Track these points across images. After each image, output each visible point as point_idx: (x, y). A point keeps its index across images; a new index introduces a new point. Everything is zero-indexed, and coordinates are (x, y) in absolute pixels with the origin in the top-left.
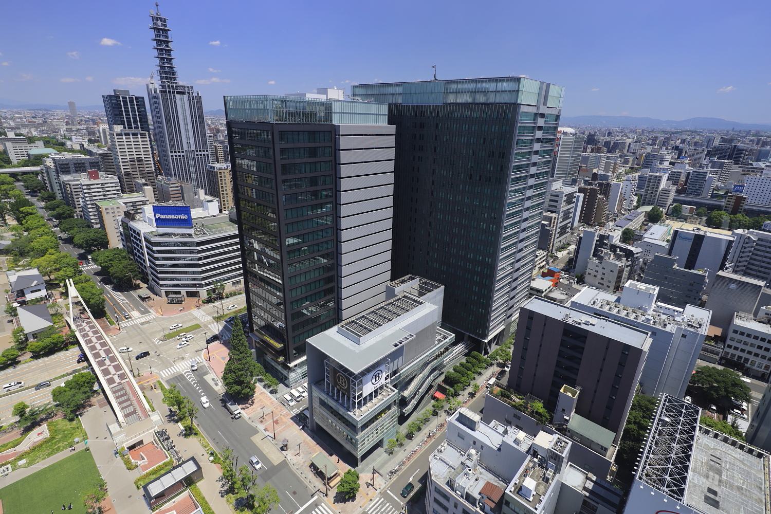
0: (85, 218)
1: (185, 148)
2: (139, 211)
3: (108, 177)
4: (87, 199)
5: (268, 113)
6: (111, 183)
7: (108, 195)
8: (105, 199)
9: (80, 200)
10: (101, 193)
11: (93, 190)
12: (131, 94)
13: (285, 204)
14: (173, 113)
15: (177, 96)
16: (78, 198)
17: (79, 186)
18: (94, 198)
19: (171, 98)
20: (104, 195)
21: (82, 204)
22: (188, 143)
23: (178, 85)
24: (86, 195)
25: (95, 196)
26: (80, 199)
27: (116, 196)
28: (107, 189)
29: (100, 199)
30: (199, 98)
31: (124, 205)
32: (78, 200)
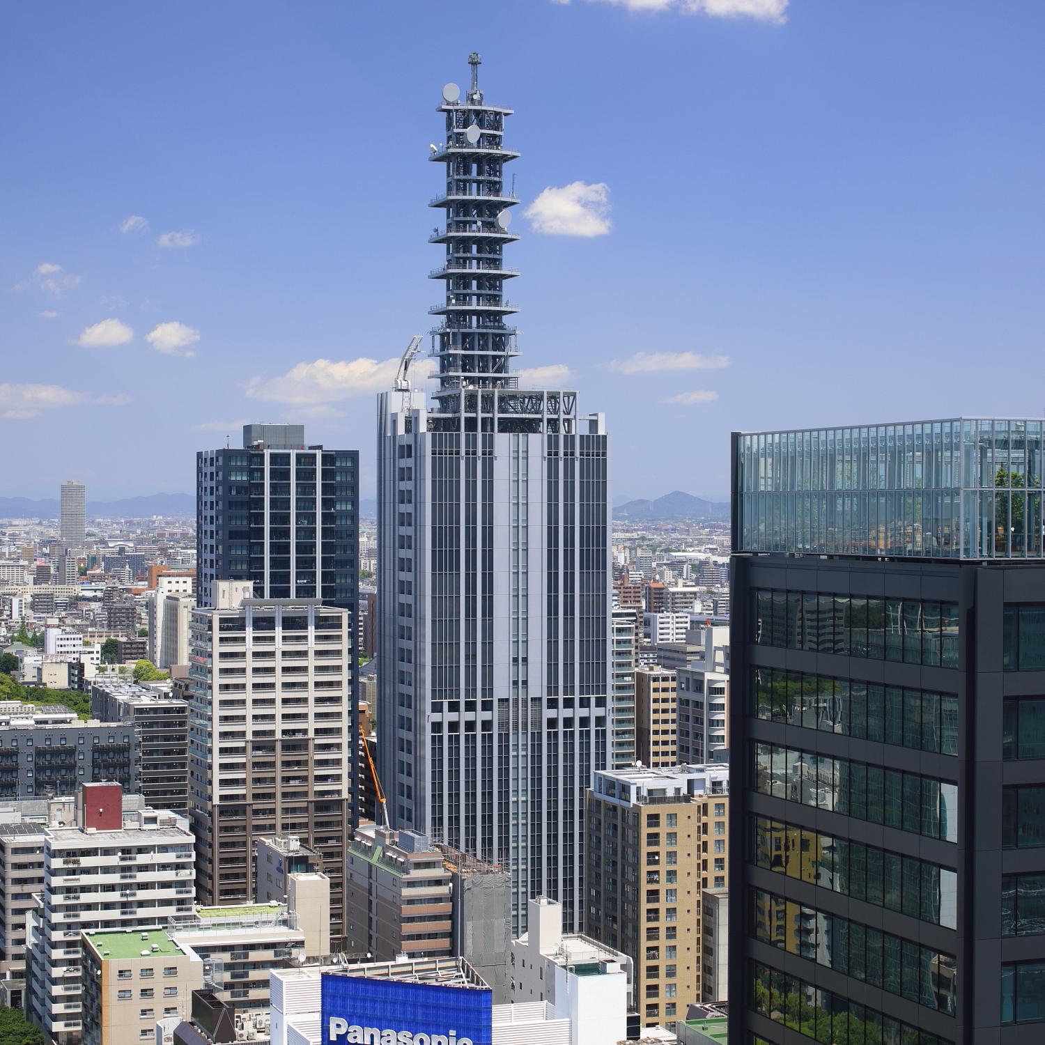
0: (31, 1008)
1: (502, 688)
2: (254, 994)
3: (154, 820)
4: (57, 918)
5: (954, 508)
6: (164, 849)
7: (141, 904)
8: (125, 923)
9: (30, 920)
10: (115, 896)
11: (85, 880)
12: (309, 440)
13: (1008, 1016)
14: (471, 518)
15: (503, 441)
16: (21, 912)
17: (37, 857)
18: (85, 916)
19: (471, 453)
20: (124, 905)
21: (31, 940)
22: (521, 661)
23: (511, 389)
24: (57, 899)
25: (89, 907)
26: (29, 915)
27: (170, 911)
28: (142, 877)
29: (107, 924)
30: (596, 446)
31: (195, 957)
32: (17, 919)
